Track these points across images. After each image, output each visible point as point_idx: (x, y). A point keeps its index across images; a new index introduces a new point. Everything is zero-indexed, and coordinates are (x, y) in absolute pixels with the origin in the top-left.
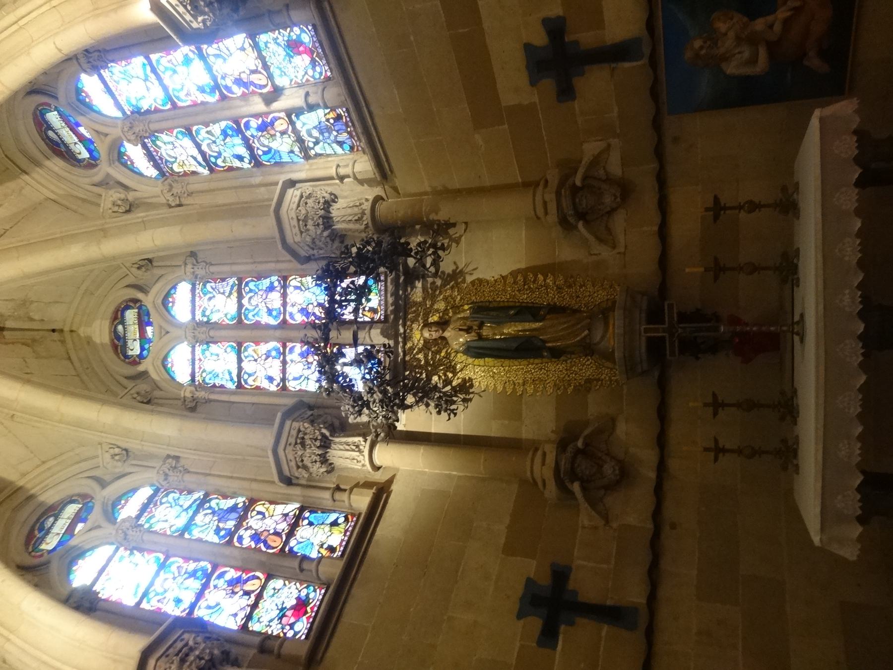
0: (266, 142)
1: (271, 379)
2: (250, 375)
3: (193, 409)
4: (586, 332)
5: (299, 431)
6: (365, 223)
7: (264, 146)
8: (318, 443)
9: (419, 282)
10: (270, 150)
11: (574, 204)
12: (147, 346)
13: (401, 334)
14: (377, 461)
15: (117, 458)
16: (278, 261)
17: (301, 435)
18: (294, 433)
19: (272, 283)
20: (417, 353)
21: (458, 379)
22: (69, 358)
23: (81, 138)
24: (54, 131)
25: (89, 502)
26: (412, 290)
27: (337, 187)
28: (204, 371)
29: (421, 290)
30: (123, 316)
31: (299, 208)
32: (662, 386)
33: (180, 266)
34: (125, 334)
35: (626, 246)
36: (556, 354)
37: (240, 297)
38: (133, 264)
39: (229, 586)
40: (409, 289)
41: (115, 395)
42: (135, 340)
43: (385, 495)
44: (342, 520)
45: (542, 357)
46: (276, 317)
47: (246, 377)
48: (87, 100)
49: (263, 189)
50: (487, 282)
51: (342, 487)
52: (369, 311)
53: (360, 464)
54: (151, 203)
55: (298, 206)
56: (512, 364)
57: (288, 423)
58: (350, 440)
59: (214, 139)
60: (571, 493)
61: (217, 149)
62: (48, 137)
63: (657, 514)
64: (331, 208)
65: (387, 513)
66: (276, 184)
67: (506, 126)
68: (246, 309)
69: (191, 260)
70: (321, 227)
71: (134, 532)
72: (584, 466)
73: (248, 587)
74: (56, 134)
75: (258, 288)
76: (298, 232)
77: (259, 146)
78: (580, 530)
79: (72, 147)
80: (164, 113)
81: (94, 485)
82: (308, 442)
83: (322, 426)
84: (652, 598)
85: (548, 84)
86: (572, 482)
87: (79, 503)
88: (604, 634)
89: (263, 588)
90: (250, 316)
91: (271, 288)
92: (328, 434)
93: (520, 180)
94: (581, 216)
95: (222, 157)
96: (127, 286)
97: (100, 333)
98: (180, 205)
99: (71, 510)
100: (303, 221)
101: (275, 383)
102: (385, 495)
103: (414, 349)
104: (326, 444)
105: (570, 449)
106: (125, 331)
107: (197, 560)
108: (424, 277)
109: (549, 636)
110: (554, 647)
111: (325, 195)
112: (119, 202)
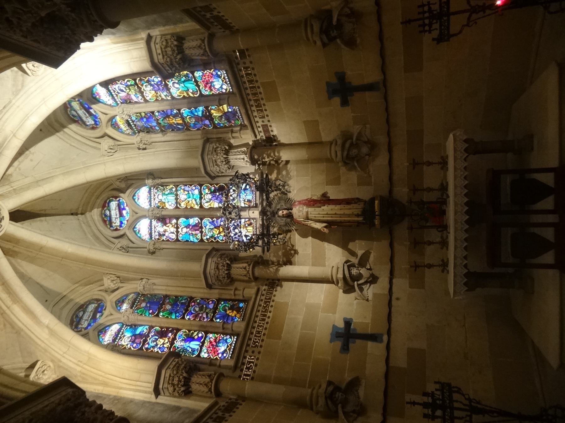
3: (153, 253)
38: (118, 179)
41: (109, 248)
48: (97, 97)
51: (238, 288)
52: (247, 202)
80: (141, 104)
81: (104, 294)
82: (221, 268)
99: (91, 307)
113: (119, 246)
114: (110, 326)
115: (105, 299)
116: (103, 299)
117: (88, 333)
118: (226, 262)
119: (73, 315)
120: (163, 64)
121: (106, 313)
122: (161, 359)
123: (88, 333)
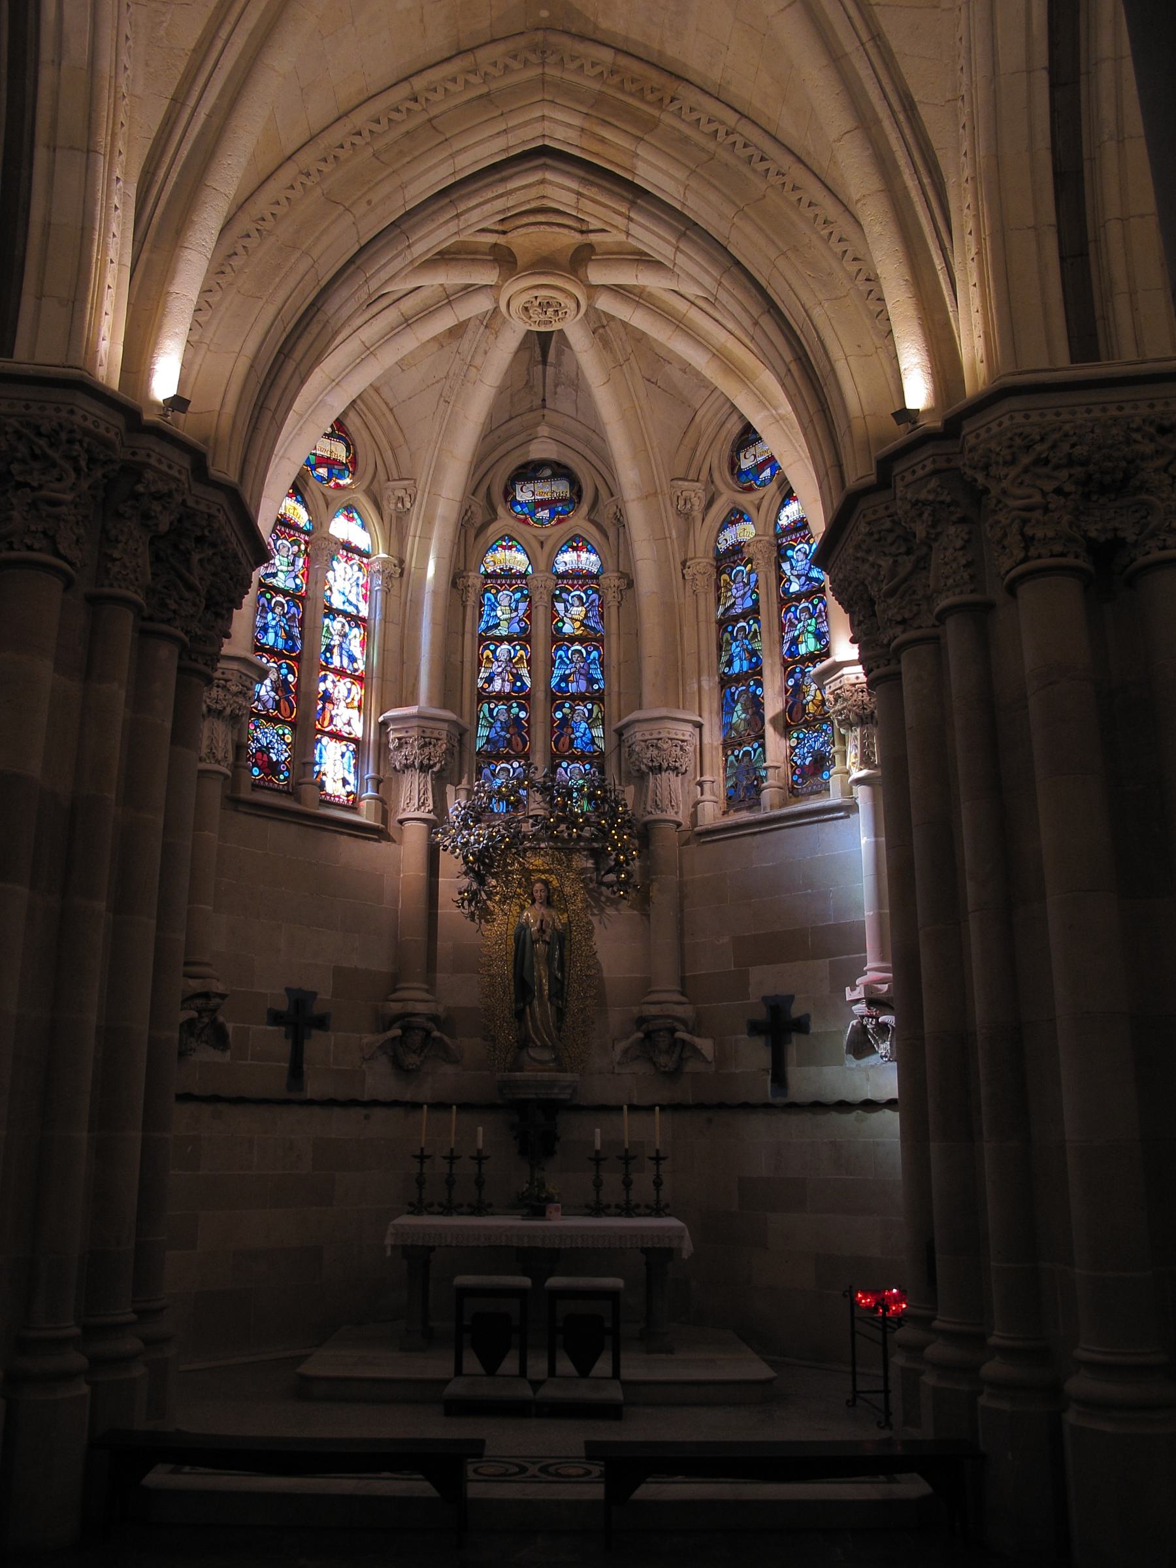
0: (742, 700)
1: (490, 680)
2: (494, 652)
3: (454, 584)
4: (539, 1043)
5: (438, 739)
6: (653, 810)
7: (739, 696)
8: (426, 762)
9: (592, 864)
10: (736, 702)
11: (660, 1030)
12: (526, 510)
13: (539, 844)
14: (408, 824)
15: (400, 505)
16: (619, 694)
17: (433, 741)
18: (436, 734)
19: (597, 681)
20: (519, 862)
21: (494, 907)
22: (511, 419)
26: (586, 856)
27: (693, 777)
28: (498, 591)
29: (585, 866)
31: (670, 741)
32: (491, 1107)
34: (541, 479)
35: (619, 1074)
36: (519, 1015)
37: (581, 640)
38: (620, 510)
39: (282, 681)
40: (585, 853)
42: (533, 494)
43: (376, 837)
44: (349, 788)
45: (516, 1001)
46: (558, 684)
47: (492, 647)
49: (696, 686)
50: (590, 939)
53: (405, 807)
54: (688, 536)
55: (671, 739)
56: (509, 963)
57: (445, 726)
58: (430, 794)
59: (749, 637)
60: (388, 1027)
61: (739, 637)
63: (375, 1103)
64: (671, 772)
65: (361, 842)
67: (733, 969)
68: (569, 648)
70: (650, 764)
71: (326, 558)
72: (417, 1038)
73: (283, 704)
75: (591, 663)
76: (646, 738)
77: (740, 689)
78: (358, 1036)
82: (427, 751)
83: (443, 763)
84: (311, 1102)
85: (762, 1014)
86: (400, 1028)
88: (282, 1064)
89: (284, 722)
90: (560, 653)
91: (591, 681)
92: (435, 769)
93: (687, 975)
94: (648, 1035)
95: (731, 641)
97: (540, 450)
100: (657, 745)
101: (486, 686)
102: (376, 837)
103: (523, 859)
104: (424, 768)
105: (430, 1025)
106: (544, 479)
107: (302, 638)
108: (597, 869)
109: (276, 1018)
110: (269, 1024)
111: (684, 767)
112: (688, 506)
118: (438, 762)
120: (841, 682)
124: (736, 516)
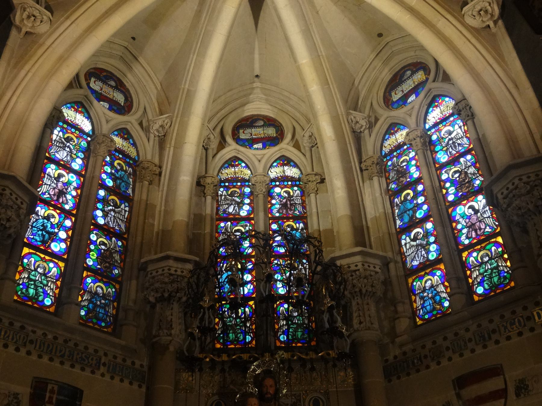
3: (198, 184)
23: (406, 96)
24: (411, 76)
25: (125, 110)
30: (270, 125)
33: (313, 171)
34: (257, 126)
62: (405, 72)
66: (386, 252)
69: (318, 178)
74: (409, 77)
79: (400, 88)
81: (140, 113)
87: (124, 103)
96: (294, 127)
98: (361, 170)
113: (212, 136)
114: (89, 118)
115: (132, 115)
116: (131, 113)
117: (81, 87)
119: (111, 73)
121: (111, 114)
122: (30, 183)
123: (81, 87)
124: (392, 129)
